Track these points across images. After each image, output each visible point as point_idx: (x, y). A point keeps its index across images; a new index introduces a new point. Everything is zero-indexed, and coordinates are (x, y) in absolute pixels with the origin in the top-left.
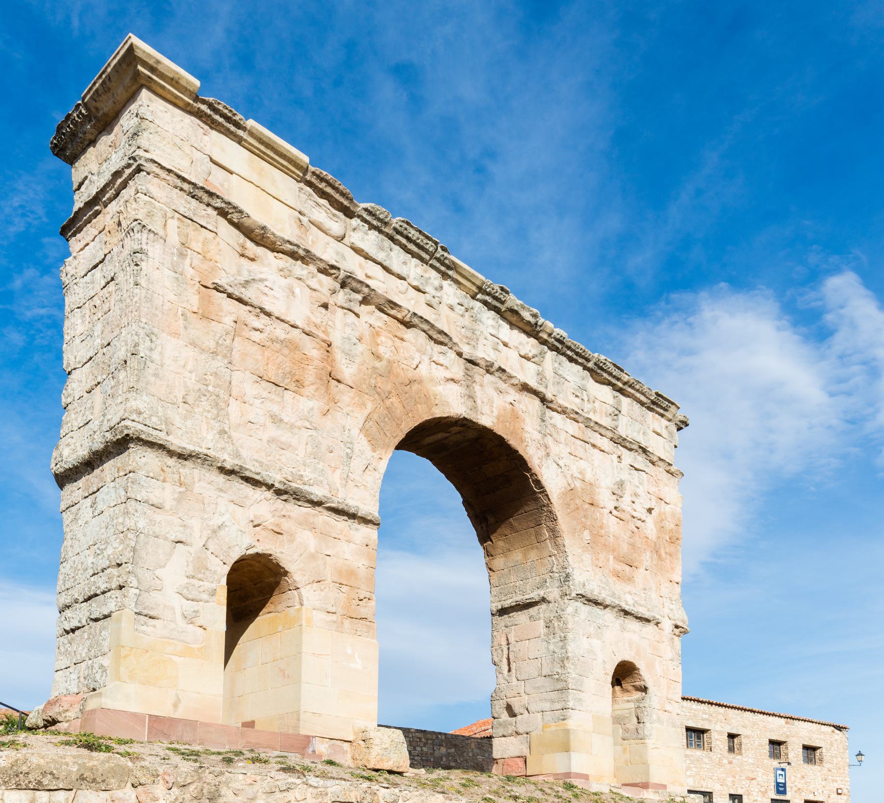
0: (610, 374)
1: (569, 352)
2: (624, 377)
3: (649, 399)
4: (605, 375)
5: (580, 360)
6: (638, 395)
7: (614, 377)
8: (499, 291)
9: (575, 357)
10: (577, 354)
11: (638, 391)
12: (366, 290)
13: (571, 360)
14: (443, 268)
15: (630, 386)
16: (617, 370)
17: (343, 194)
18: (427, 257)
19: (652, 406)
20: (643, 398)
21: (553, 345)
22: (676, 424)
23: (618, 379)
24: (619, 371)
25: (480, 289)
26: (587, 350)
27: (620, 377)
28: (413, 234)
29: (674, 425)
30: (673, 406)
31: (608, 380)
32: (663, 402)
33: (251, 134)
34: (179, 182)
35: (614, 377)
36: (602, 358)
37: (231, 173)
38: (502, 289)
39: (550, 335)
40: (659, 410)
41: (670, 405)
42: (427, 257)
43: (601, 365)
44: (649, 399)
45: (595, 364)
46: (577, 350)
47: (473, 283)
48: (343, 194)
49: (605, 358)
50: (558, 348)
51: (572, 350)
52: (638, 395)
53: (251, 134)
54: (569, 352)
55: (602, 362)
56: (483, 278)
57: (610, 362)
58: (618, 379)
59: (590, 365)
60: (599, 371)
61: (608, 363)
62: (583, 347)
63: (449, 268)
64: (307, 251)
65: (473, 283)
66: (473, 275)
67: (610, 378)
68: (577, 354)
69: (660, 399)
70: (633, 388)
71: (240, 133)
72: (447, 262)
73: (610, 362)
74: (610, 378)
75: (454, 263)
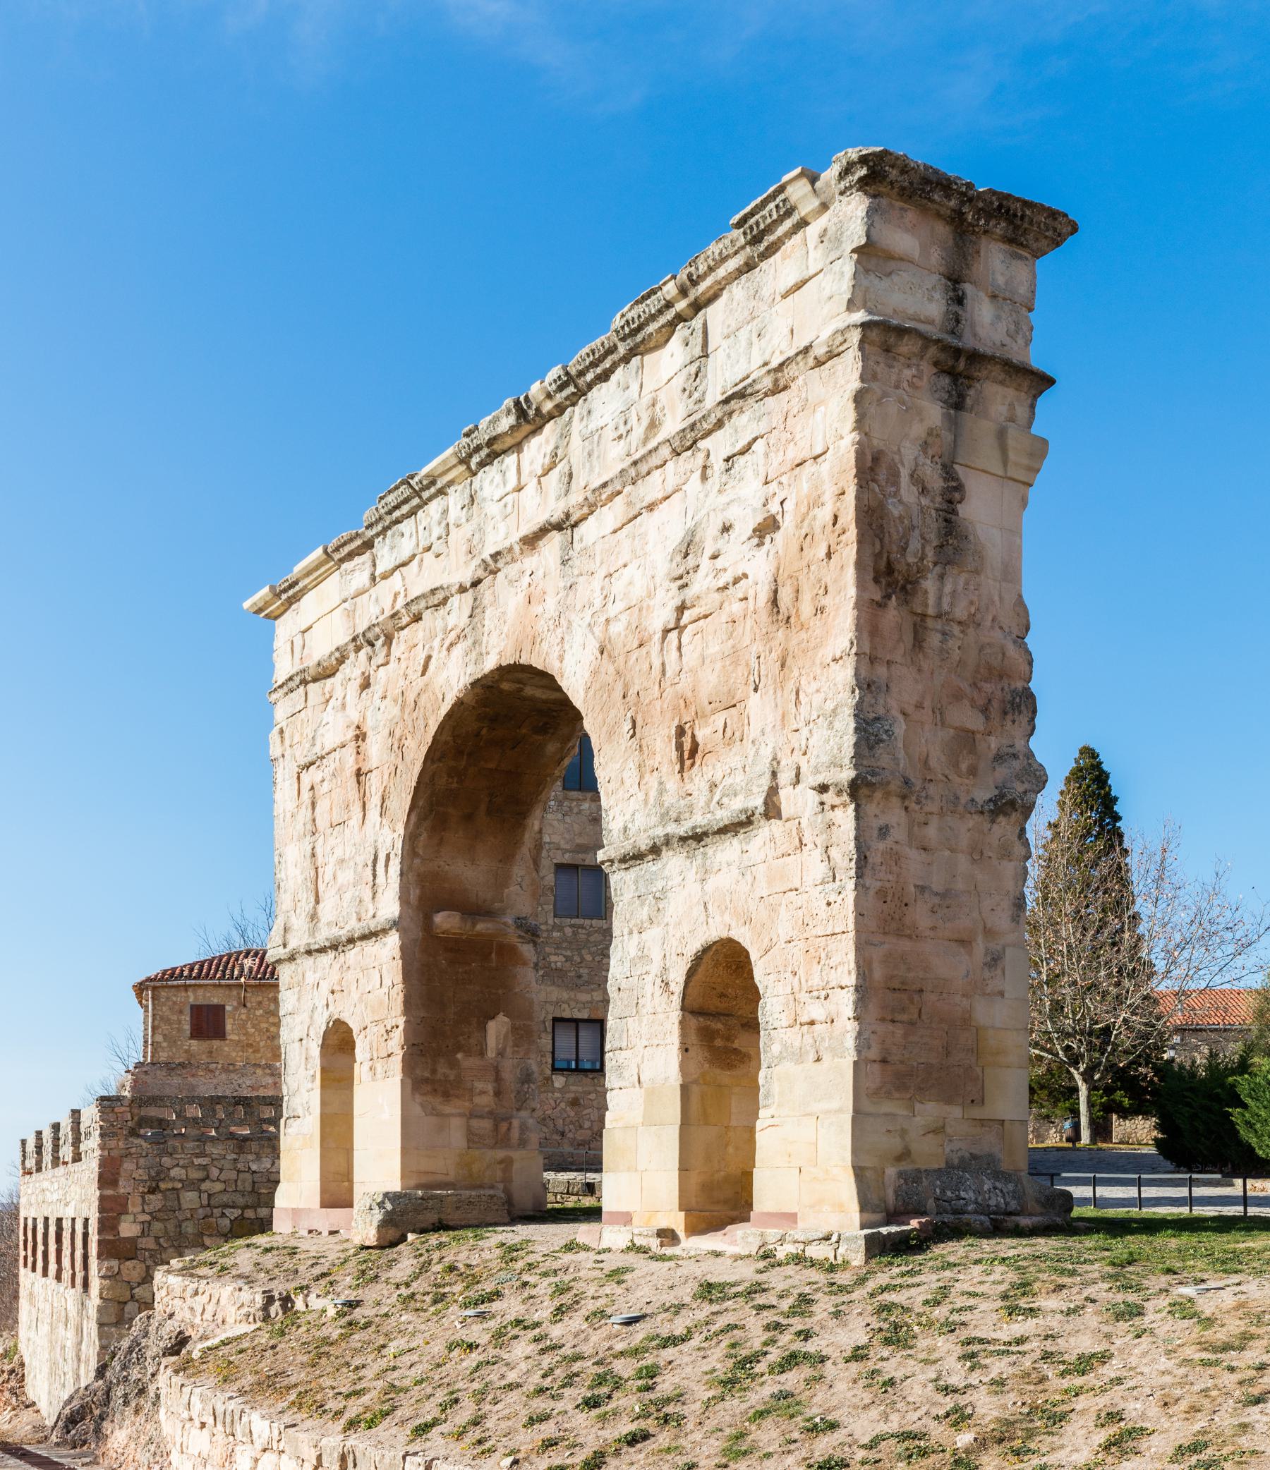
0: (653, 318)
1: (590, 376)
2: (668, 292)
3: (743, 248)
4: (652, 328)
5: (607, 364)
6: (721, 272)
7: (660, 312)
8: (468, 440)
9: (599, 370)
10: (594, 365)
11: (711, 269)
12: (377, 630)
13: (605, 377)
14: (433, 490)
15: (694, 283)
16: (648, 302)
17: (351, 540)
18: (416, 501)
19: (762, 247)
20: (732, 264)
21: (567, 398)
22: (842, 193)
23: (669, 305)
24: (653, 297)
25: (464, 461)
26: (593, 345)
27: (663, 302)
28: (392, 499)
29: (844, 199)
30: (789, 189)
31: (663, 326)
32: (764, 218)
33: (308, 574)
34: (285, 689)
35: (660, 312)
36: (618, 322)
37: (310, 627)
38: (467, 435)
39: (549, 396)
40: (781, 230)
41: (782, 197)
42: (416, 501)
43: (627, 330)
44: (743, 248)
45: (623, 339)
46: (587, 363)
47: (454, 466)
48: (351, 540)
49: (618, 316)
50: (573, 394)
51: (587, 369)
52: (721, 272)
53: (308, 574)
54: (590, 376)
55: (623, 327)
56: (450, 451)
57: (630, 310)
58: (669, 305)
59: (622, 349)
60: (639, 338)
61: (629, 316)
62: (586, 350)
63: (433, 483)
64: (338, 649)
65: (454, 466)
66: (444, 461)
67: (662, 320)
68: (594, 365)
69: (752, 221)
70: (702, 278)
71: (301, 585)
72: (425, 482)
73: (630, 310)
74: (662, 320)
75: (427, 476)
